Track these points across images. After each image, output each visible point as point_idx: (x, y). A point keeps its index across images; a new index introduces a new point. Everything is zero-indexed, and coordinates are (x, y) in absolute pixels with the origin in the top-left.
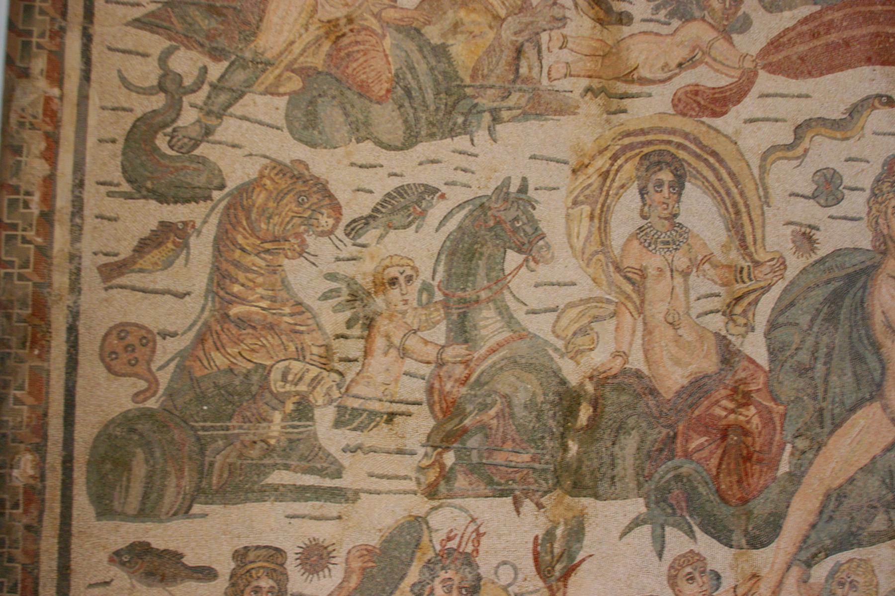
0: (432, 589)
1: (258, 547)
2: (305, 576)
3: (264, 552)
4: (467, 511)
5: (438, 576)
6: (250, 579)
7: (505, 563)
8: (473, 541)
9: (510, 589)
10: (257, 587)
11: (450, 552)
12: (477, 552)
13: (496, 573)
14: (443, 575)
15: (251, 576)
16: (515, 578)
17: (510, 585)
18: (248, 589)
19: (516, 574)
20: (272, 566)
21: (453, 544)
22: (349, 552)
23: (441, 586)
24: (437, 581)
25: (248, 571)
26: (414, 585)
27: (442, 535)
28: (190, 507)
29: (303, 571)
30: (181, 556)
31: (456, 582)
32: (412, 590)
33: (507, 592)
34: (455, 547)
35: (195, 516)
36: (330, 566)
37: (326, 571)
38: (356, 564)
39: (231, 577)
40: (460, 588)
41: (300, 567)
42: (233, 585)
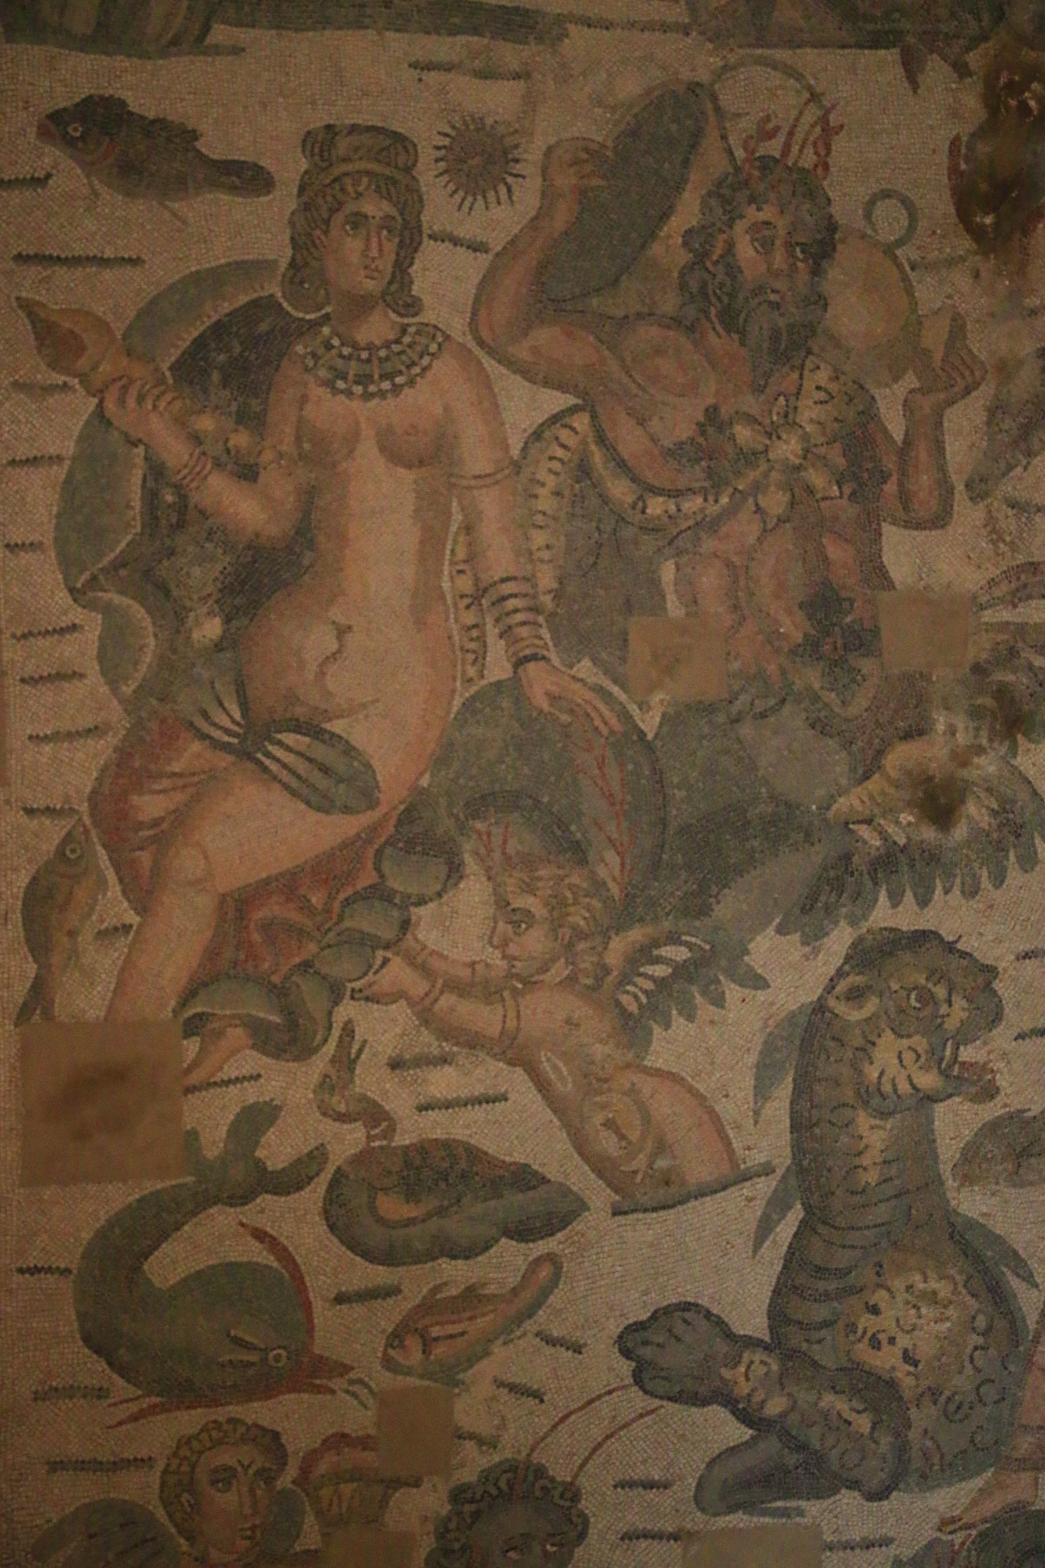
0: (730, 246)
1: (354, 129)
2: (458, 198)
3: (366, 139)
4: (799, 77)
5: (742, 217)
6: (340, 196)
7: (886, 194)
8: (815, 144)
9: (899, 252)
10: (357, 214)
11: (766, 164)
12: (826, 167)
13: (868, 216)
14: (751, 211)
15: (343, 190)
16: (912, 228)
17: (900, 243)
18: (339, 218)
19: (913, 218)
20: (387, 172)
21: (773, 148)
22: (550, 150)
23: (748, 237)
24: (740, 226)
25: (335, 180)
26: (689, 232)
27: (747, 125)
28: (206, 29)
29: (452, 187)
30: (194, 135)
31: (782, 232)
32: (685, 244)
33: (895, 258)
34: (777, 154)
35: (217, 50)
36: (510, 179)
37: (503, 190)
38: (566, 180)
39: (302, 189)
40: (789, 246)
41: (446, 178)
42: (307, 207)
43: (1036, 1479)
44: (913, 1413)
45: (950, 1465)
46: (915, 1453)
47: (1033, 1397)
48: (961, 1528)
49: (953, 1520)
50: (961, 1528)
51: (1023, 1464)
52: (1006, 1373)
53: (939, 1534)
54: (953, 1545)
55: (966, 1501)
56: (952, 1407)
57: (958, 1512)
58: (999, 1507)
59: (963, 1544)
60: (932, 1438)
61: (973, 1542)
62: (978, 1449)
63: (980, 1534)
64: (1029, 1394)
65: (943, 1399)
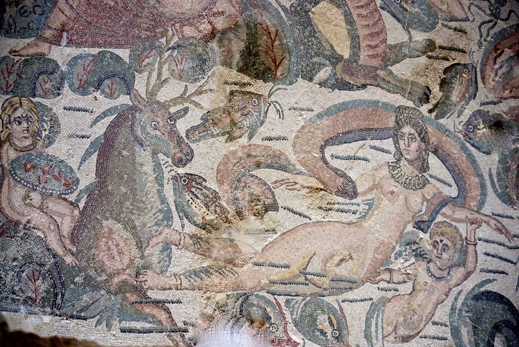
43: (50, 47)
44: (8, 8)
45: (18, 31)
46: (6, 23)
47: (54, 17)
48: (18, 55)
49: (15, 51)
50: (18, 55)
51: (46, 40)
52: (46, 5)
53: (9, 55)
54: (14, 60)
55: (21, 46)
56: (22, 11)
57: (18, 49)
58: (35, 52)
59: (18, 61)
60: (13, 19)
61: (22, 62)
62: (30, 29)
63: (25, 60)
64: (53, 16)
65: (20, 6)
